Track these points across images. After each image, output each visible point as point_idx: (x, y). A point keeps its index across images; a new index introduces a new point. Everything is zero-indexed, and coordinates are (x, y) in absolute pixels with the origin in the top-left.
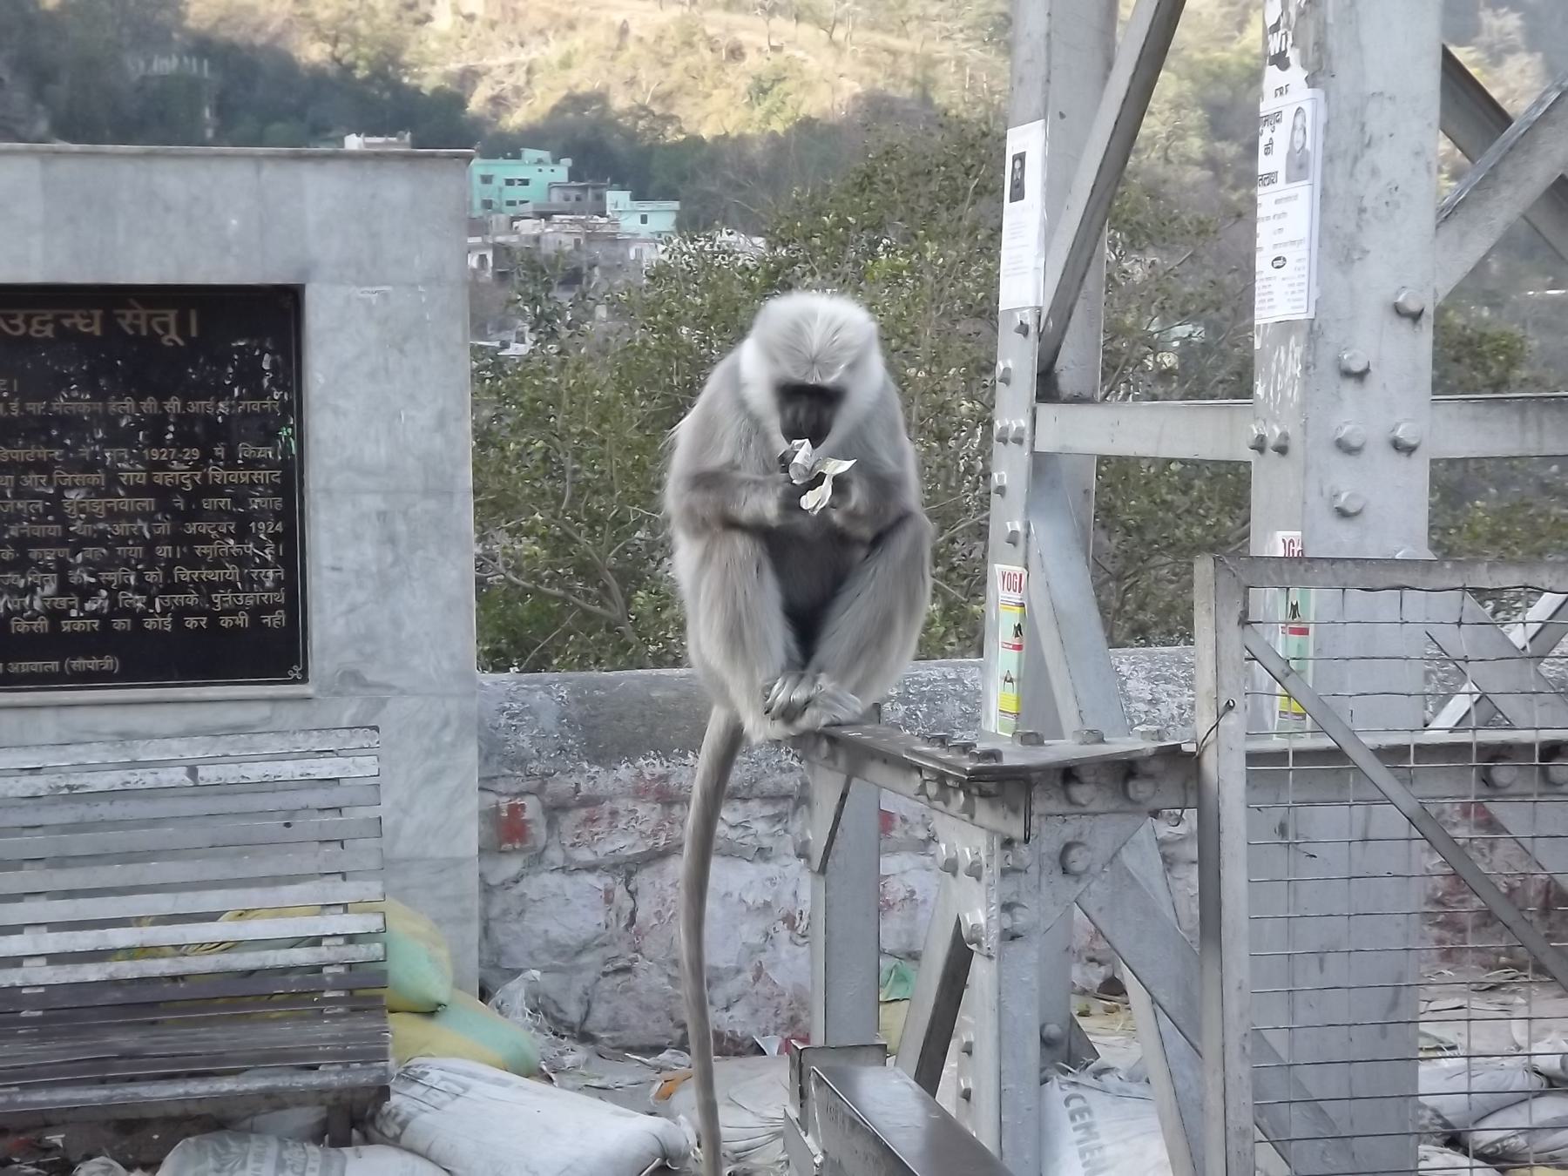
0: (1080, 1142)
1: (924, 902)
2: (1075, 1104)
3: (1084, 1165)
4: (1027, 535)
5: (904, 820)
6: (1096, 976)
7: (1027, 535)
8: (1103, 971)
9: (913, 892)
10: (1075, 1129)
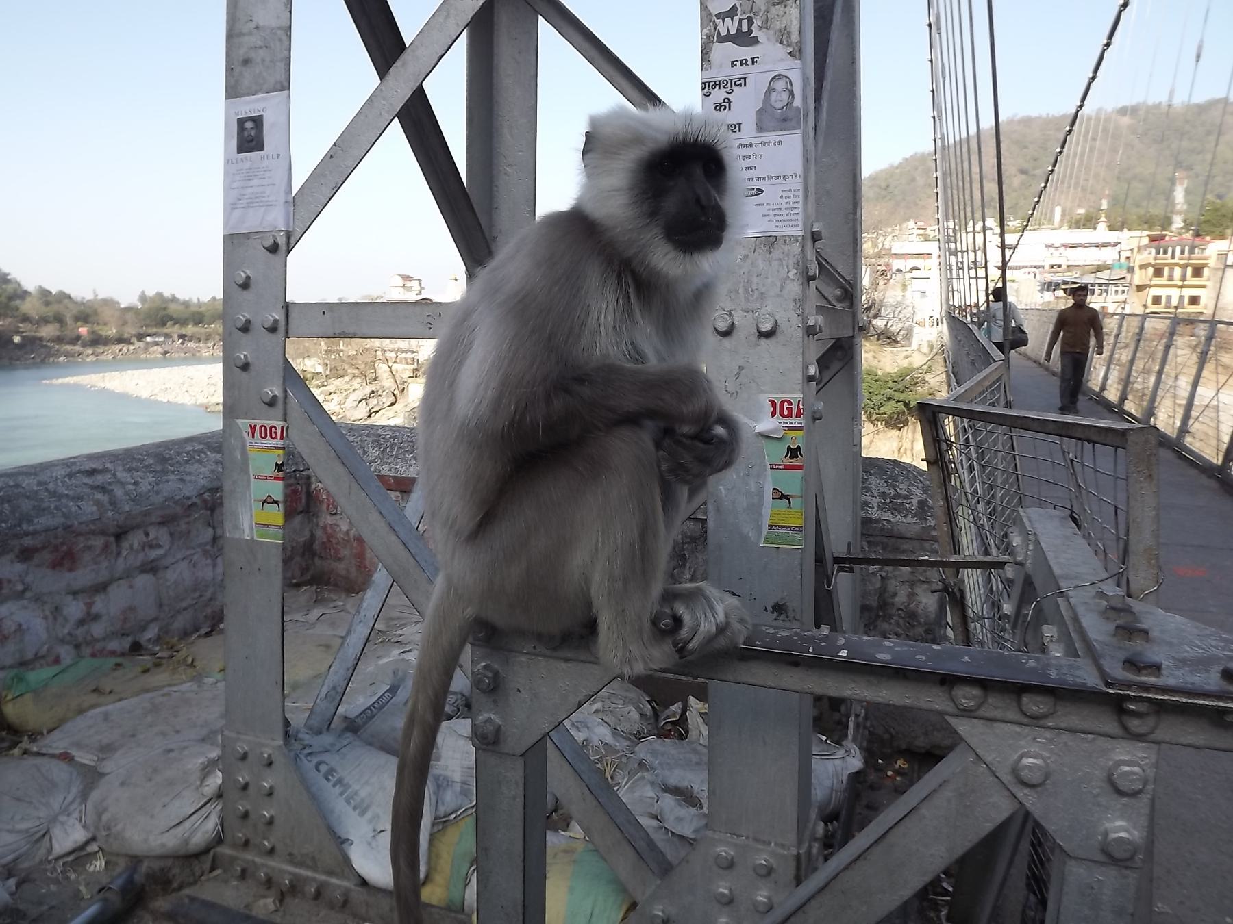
0: (341, 794)
1: (28, 629)
2: (323, 768)
3: (355, 808)
4: (286, 397)
5: (9, 581)
6: (126, 643)
7: (286, 397)
8: (130, 639)
9: (20, 625)
10: (334, 786)
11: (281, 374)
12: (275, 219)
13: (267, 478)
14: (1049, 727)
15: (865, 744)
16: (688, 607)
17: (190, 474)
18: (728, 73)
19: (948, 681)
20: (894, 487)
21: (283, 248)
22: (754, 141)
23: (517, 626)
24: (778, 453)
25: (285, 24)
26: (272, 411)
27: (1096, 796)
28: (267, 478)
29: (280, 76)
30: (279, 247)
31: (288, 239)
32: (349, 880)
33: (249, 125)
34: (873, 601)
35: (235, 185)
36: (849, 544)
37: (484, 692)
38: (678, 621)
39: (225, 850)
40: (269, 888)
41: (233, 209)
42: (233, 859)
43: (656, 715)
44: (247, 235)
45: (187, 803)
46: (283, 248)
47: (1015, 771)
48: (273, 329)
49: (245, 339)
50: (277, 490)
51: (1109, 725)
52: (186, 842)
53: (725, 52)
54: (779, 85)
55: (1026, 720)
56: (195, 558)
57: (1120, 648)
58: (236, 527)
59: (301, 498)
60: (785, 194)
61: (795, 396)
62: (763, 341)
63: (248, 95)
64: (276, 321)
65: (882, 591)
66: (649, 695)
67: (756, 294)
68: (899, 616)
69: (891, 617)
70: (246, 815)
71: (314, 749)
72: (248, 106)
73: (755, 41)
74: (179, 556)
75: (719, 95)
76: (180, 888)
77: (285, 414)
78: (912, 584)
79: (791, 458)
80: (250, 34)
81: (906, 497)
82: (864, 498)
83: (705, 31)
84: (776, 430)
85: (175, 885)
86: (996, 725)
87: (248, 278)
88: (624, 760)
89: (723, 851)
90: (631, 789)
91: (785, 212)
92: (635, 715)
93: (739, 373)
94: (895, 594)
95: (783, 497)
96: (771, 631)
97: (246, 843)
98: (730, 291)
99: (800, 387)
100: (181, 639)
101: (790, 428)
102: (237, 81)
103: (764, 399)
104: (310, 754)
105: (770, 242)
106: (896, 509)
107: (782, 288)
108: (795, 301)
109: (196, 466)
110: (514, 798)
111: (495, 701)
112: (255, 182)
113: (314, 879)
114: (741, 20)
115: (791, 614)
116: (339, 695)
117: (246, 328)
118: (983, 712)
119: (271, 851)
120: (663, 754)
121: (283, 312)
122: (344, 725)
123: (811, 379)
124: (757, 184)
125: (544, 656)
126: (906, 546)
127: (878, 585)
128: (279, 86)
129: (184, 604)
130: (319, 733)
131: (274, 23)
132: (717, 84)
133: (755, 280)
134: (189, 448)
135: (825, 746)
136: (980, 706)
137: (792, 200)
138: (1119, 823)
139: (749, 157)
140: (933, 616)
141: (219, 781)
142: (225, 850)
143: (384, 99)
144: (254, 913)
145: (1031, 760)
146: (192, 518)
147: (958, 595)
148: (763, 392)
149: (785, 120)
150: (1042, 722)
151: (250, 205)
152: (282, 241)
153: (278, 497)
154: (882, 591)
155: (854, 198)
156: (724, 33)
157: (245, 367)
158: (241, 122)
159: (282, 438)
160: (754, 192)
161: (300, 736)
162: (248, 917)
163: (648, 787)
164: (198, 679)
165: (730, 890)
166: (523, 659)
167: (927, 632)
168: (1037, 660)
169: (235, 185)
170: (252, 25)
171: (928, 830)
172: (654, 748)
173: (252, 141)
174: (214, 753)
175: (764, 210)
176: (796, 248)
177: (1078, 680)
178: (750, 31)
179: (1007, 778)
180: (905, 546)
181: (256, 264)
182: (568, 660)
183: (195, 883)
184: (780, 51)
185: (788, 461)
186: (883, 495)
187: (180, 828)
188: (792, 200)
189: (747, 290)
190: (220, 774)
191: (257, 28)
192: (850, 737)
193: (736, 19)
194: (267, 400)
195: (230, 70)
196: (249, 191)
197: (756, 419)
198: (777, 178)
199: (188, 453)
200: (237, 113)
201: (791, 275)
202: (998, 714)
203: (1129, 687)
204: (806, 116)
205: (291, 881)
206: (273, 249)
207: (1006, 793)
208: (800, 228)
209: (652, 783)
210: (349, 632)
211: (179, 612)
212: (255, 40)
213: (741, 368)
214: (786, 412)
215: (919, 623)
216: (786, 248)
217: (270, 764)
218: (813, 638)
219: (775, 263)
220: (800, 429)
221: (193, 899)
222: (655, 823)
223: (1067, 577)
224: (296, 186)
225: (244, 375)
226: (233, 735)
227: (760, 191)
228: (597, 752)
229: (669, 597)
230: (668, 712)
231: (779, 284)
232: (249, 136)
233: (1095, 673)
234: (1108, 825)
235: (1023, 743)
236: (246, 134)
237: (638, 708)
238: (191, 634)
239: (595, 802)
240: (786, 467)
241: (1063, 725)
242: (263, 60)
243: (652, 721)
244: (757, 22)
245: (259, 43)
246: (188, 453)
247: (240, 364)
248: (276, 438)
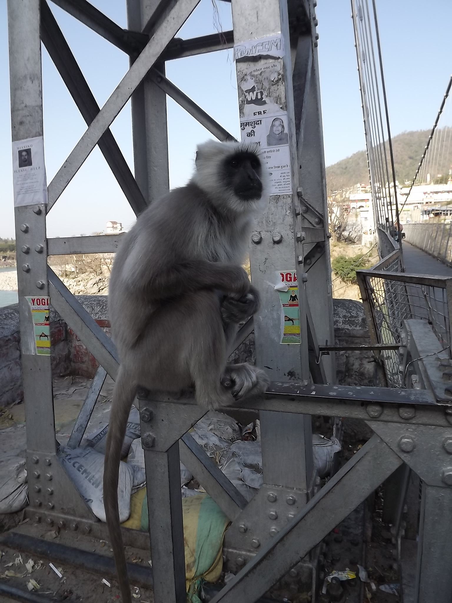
0: (86, 477)
2: (77, 465)
3: (93, 484)
4: (48, 284)
7: (48, 284)
10: (82, 474)
11: (46, 273)
12: (39, 198)
13: (41, 324)
14: (414, 424)
15: (342, 438)
16: (238, 375)
17: (7, 324)
18: (253, 118)
19: (364, 404)
20: (350, 313)
21: (44, 212)
22: (266, 150)
23: (160, 388)
24: (286, 299)
25: (40, 104)
26: (42, 292)
27: (438, 455)
28: (41, 324)
29: (38, 129)
30: (42, 212)
31: (46, 207)
32: (91, 519)
33: (24, 153)
34: (343, 369)
35: (19, 183)
36: (327, 341)
37: (146, 422)
38: (233, 382)
39: (30, 509)
40: (53, 526)
41: (19, 194)
42: (34, 513)
43: (241, 429)
44: (26, 207)
45: (10, 487)
46: (44, 212)
47: (399, 445)
48: (41, 252)
49: (27, 257)
50: (46, 330)
51: (441, 420)
52: (11, 506)
53: (251, 108)
54: (277, 123)
55: (402, 421)
56: (11, 366)
57: (444, 384)
58: (28, 349)
59: (60, 333)
60: (282, 175)
61: (293, 271)
62: (276, 246)
63: (23, 139)
64: (42, 248)
65: (347, 364)
66: (237, 420)
67: (271, 223)
68: (356, 375)
69: (352, 376)
70: (39, 491)
71: (72, 456)
72: (24, 144)
73: (264, 103)
74: (3, 365)
75: (249, 129)
76: (9, 529)
77: (49, 293)
78: (361, 359)
79: (293, 301)
80: (23, 109)
81: (356, 317)
82: (335, 319)
83: (241, 99)
84: (284, 288)
85: (6, 528)
86: (389, 423)
87: (27, 227)
88: (225, 452)
89: (271, 493)
90: (229, 467)
91: (283, 183)
92: (230, 430)
93: (265, 261)
94: (353, 365)
95: (289, 320)
96: (280, 384)
97: (41, 505)
98: (259, 222)
99: (294, 267)
100: (6, 406)
101: (291, 287)
102: (17, 133)
103: (278, 273)
104: (70, 458)
105: (277, 198)
106: (351, 323)
107: (284, 220)
108: (290, 225)
109: (10, 320)
110: (164, 473)
111: (152, 426)
112: (29, 181)
113: (74, 520)
114: (257, 93)
115: (297, 376)
116: (83, 429)
117: (27, 252)
118: (383, 418)
119: (53, 508)
120: (244, 449)
121: (45, 243)
122: (87, 444)
123: (300, 262)
125: (174, 403)
126: (357, 341)
127: (345, 360)
128: (38, 134)
129: (7, 389)
130: (74, 448)
131: (34, 104)
132: (247, 124)
133: (271, 216)
134: (6, 312)
135: (322, 440)
136: (380, 415)
137: (286, 177)
138: (449, 468)
140: (372, 374)
141: (26, 475)
142: (30, 509)
143: (89, 138)
144: (45, 539)
145: (406, 440)
146: (9, 347)
147: (381, 363)
149: (280, 140)
150: (410, 421)
151: (26, 192)
152: (43, 209)
153: (47, 333)
154: (347, 364)
155: (322, 175)
156: (249, 99)
157: (28, 271)
158: (20, 152)
159: (48, 304)
161: (65, 450)
162: (42, 541)
163: (237, 465)
164: (15, 425)
165: (276, 512)
166: (164, 405)
167: (370, 382)
168: (406, 391)
169: (19, 183)
170: (23, 105)
171: (364, 476)
172: (239, 446)
173: (26, 161)
174: (23, 462)
176: (289, 200)
177: (424, 400)
178: (262, 98)
179: (396, 449)
180: (356, 341)
181: (31, 221)
182: (185, 404)
183: (16, 526)
184: (277, 107)
185: (291, 302)
186: (345, 317)
187: (8, 499)
188: (286, 177)
189: (267, 221)
190: (26, 472)
191: (26, 106)
192: (334, 435)
193: (255, 93)
194: (39, 286)
195: (13, 127)
196: (26, 185)
197: (275, 283)
198: (279, 167)
199: (5, 315)
200: (18, 148)
201: (287, 213)
202: (389, 418)
203: (447, 402)
204: (291, 137)
205: (63, 522)
206: (39, 213)
207: (396, 456)
208: (291, 190)
209: (239, 463)
210: (87, 398)
211: (4, 393)
212: (25, 112)
213: (266, 259)
214: (289, 279)
215: (366, 378)
216: (284, 200)
217: (50, 465)
218: (300, 386)
220: (296, 286)
221: (15, 534)
222: (241, 482)
223: (424, 351)
224: (48, 184)
225: (28, 275)
226: (31, 451)
228: (212, 449)
229: (229, 370)
230: (246, 428)
231: (282, 218)
232: (25, 159)
233: (433, 396)
234: (444, 469)
235: (402, 432)
236: (23, 158)
237: (231, 427)
238: (11, 403)
239: (209, 474)
240: (290, 305)
241: (420, 422)
242: (29, 122)
243: (239, 433)
244: (265, 94)
245: (27, 114)
246: (5, 315)
247: (25, 270)
248: (45, 304)
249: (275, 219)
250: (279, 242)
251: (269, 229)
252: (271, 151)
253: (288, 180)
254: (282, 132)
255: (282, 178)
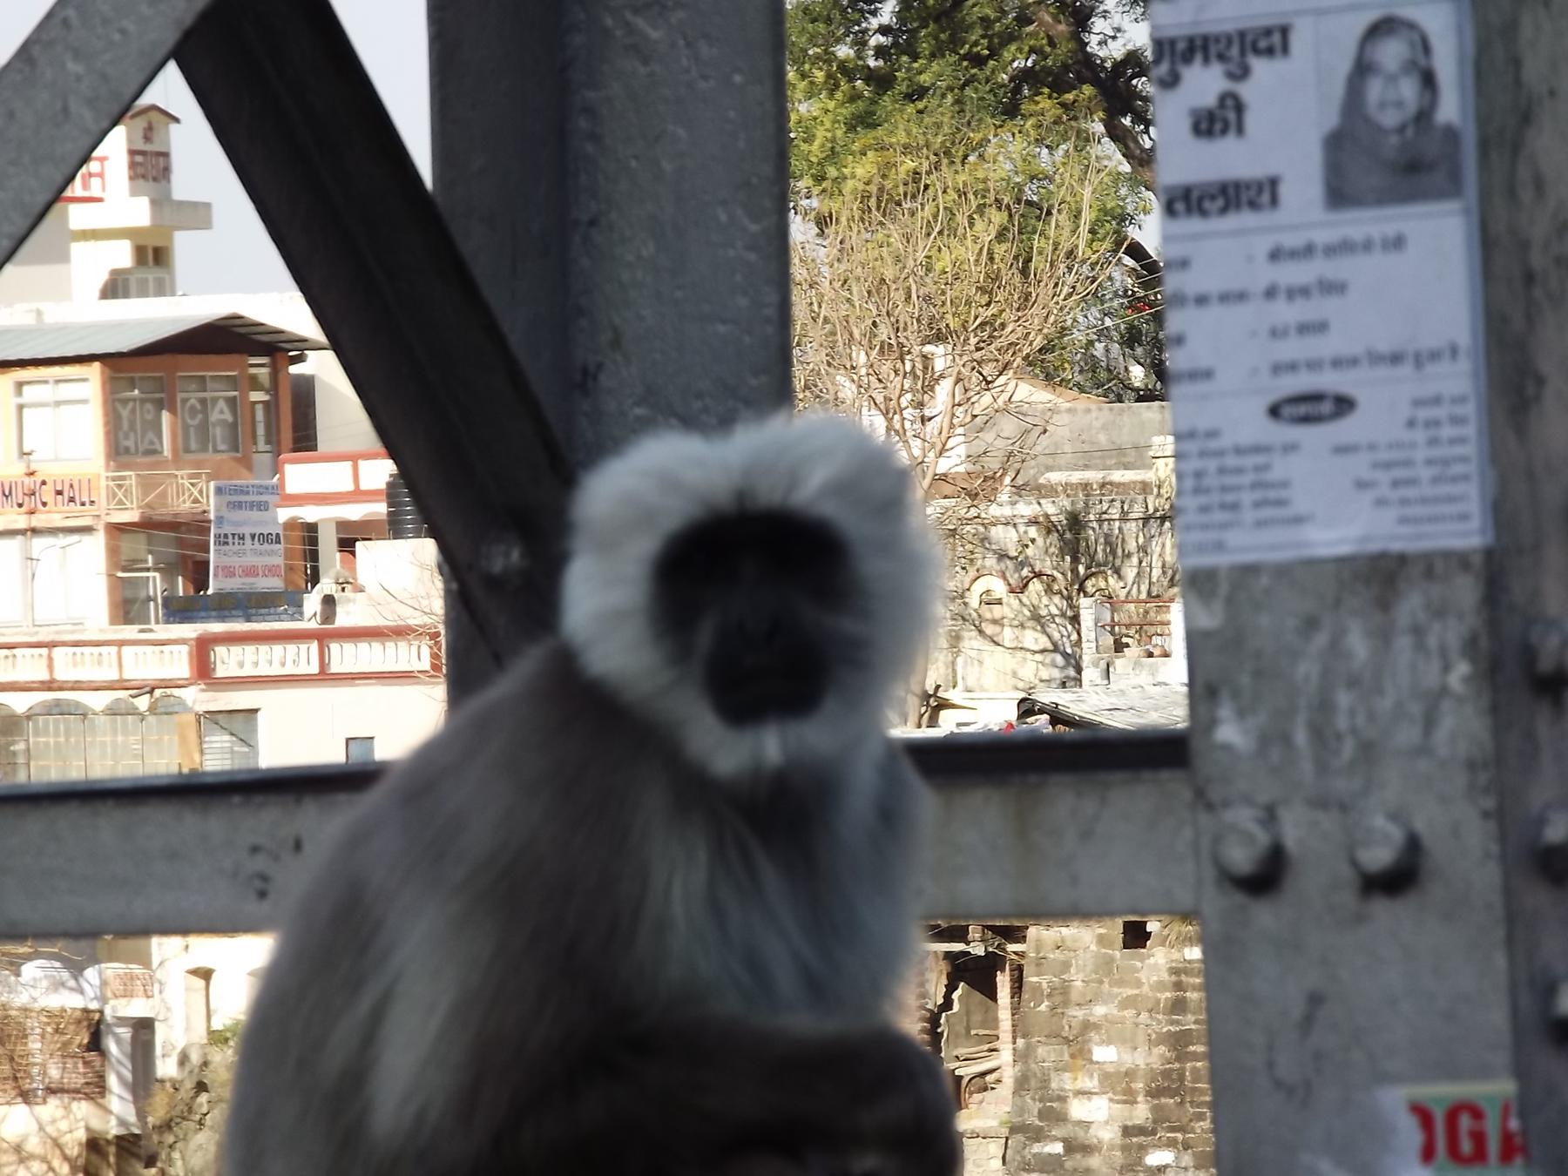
22: (1322, 237)
54: (1391, 53)
60: (1424, 414)
62: (1383, 910)
67: (1348, 749)
91: (1425, 473)
98: (1264, 742)
99: (1502, 1058)
103: (1394, 1100)
105: (1381, 576)
107: (1429, 723)
108: (1471, 766)
124: (1329, 381)
133: (1344, 699)
137: (1447, 431)
139: (1305, 292)
143: (77, 55)
148: (1385, 1078)
160: (1326, 407)
175: (1359, 465)
176: (1466, 591)
188: (1447, 431)
189: (1321, 735)
198: (1396, 359)
208: (1475, 523)
213: (1315, 1000)
214: (1466, 1146)
219: (1403, 643)
227: (1344, 405)
231: (1416, 709)
249: (1371, 717)
250: (1398, 879)
251: (1341, 785)
252: (1344, 248)
253: (1459, 450)
254: (1424, 116)
255: (1420, 435)
